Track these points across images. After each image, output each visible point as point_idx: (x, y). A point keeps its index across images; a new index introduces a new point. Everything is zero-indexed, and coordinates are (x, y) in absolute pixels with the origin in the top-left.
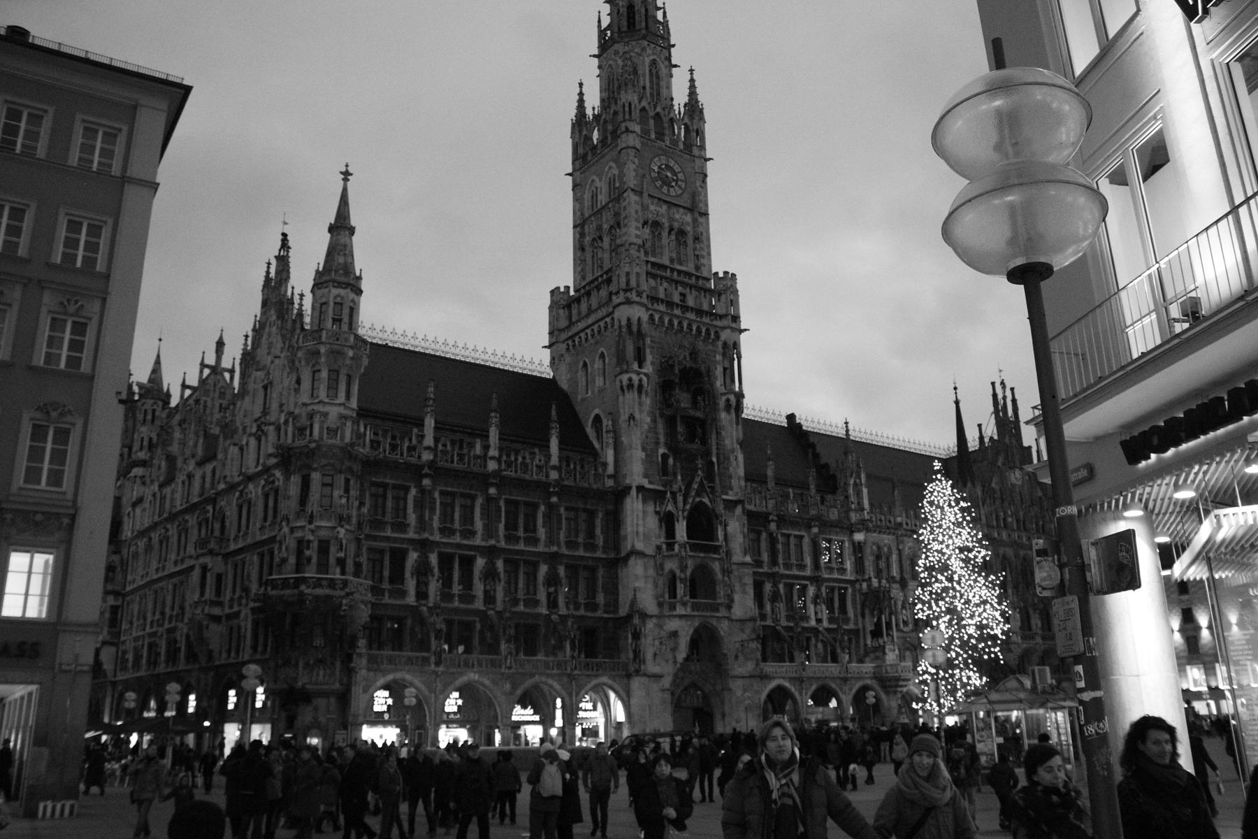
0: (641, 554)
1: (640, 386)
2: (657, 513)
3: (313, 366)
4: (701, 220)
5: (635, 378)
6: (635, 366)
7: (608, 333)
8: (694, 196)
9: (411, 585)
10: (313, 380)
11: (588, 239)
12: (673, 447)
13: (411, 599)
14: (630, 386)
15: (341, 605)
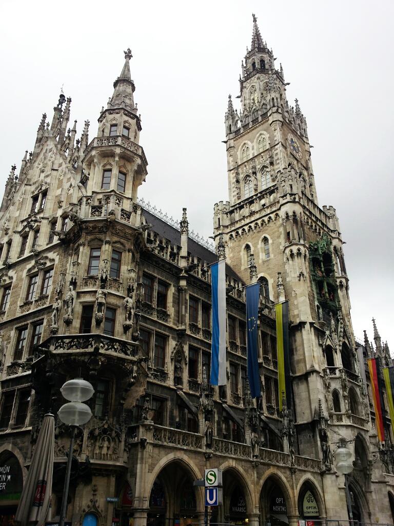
0: (318, 373)
1: (305, 256)
2: (320, 345)
3: (104, 166)
4: (312, 176)
5: (303, 249)
6: (302, 242)
7: (271, 224)
8: (307, 162)
9: (170, 368)
10: (103, 177)
11: (241, 176)
12: (324, 305)
13: (170, 383)
14: (299, 254)
15: (132, 372)
